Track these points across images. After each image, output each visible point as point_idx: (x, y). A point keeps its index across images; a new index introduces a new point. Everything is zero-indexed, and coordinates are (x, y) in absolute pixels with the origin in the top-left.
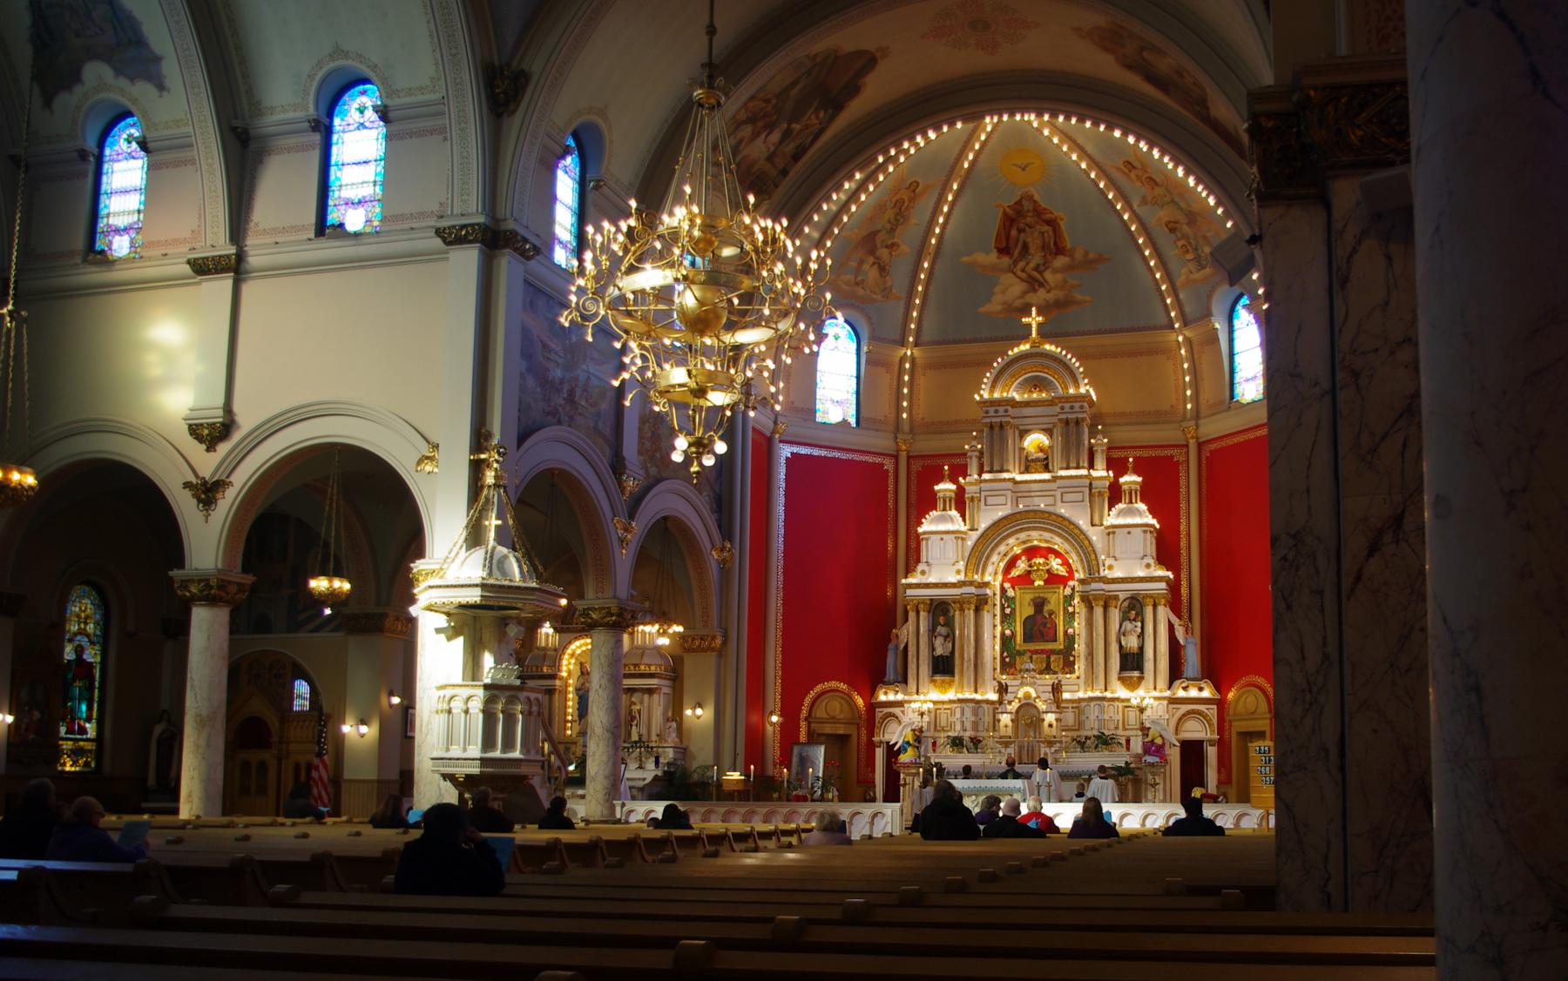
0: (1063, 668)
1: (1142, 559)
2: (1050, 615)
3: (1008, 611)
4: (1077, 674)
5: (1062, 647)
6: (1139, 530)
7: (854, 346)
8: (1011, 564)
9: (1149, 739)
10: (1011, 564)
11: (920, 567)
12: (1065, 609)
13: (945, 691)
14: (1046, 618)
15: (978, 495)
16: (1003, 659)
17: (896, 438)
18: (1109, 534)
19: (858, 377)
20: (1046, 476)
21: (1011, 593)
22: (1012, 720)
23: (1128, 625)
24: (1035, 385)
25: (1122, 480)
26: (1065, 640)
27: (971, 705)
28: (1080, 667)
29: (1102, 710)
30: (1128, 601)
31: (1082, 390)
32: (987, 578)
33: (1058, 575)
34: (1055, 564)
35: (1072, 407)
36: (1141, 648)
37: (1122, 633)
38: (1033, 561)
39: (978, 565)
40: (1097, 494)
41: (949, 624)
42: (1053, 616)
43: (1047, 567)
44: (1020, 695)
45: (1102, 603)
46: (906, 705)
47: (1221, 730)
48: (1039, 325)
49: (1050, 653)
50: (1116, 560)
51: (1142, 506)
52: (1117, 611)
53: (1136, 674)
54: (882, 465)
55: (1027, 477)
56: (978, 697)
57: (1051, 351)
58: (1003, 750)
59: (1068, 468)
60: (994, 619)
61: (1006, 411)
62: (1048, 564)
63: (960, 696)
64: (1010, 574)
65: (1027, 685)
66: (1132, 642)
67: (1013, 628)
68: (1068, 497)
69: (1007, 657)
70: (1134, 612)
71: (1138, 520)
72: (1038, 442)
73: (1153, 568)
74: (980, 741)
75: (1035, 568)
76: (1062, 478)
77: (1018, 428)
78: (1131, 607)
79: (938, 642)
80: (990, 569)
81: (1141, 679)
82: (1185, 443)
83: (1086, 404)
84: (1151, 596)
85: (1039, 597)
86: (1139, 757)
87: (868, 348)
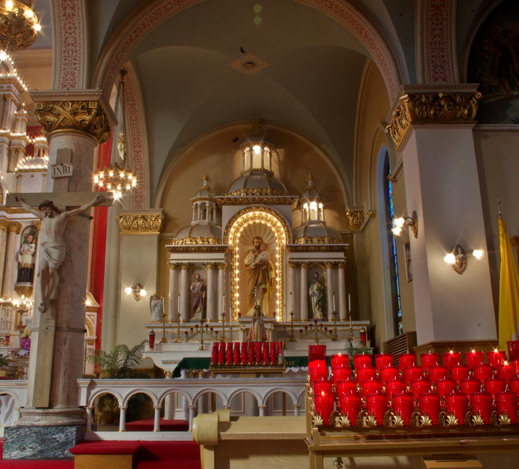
6: (40, 174)
23: (26, 247)
36: (34, 265)
52: (19, 236)
53: (28, 284)
66: (27, 260)
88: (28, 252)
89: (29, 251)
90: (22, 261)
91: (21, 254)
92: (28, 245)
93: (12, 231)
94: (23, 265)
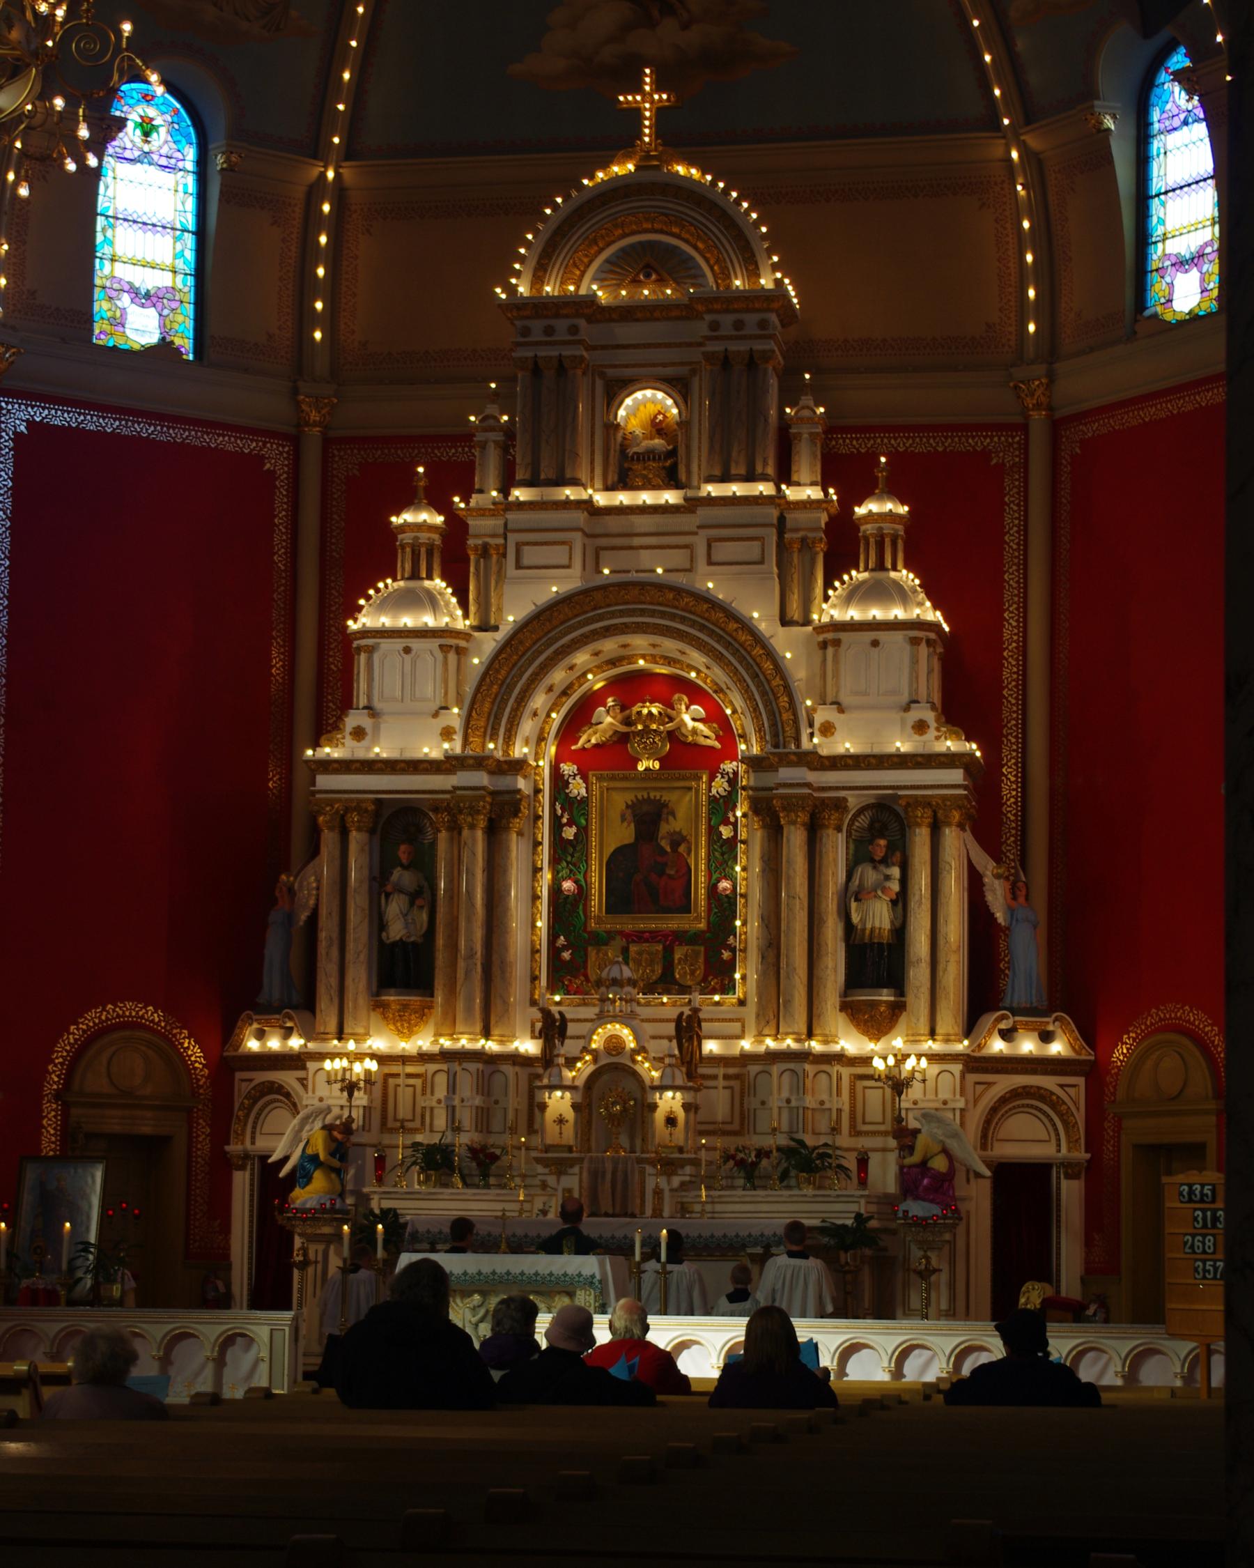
0: (705, 979)
1: (907, 709)
2: (675, 844)
3: (569, 833)
4: (739, 992)
5: (702, 925)
6: (899, 637)
7: (191, 153)
8: (579, 717)
9: (916, 1158)
10: (579, 717)
11: (352, 720)
12: (713, 832)
13: (407, 1031)
14: (662, 852)
15: (501, 541)
16: (554, 952)
17: (295, 391)
18: (824, 645)
19: (200, 233)
20: (670, 497)
21: (578, 788)
22: (575, 1106)
23: (869, 875)
24: (648, 266)
25: (860, 511)
26: (709, 909)
27: (473, 1067)
28: (746, 976)
29: (799, 1086)
30: (868, 814)
31: (766, 282)
32: (520, 750)
33: (695, 745)
34: (690, 718)
35: (739, 325)
36: (900, 932)
37: (852, 894)
38: (635, 709)
39: (498, 718)
40: (796, 546)
41: (424, 863)
42: (682, 849)
43: (670, 726)
44: (597, 1042)
45: (803, 817)
46: (312, 1066)
47: (1093, 1140)
48: (661, 113)
49: (674, 939)
50: (841, 710)
51: (906, 577)
52: (841, 838)
53: (886, 996)
54: (261, 459)
55: (623, 498)
56: (492, 1046)
57: (689, 179)
58: (552, 1180)
59: (725, 478)
60: (534, 852)
61: (574, 330)
62: (671, 719)
63: (446, 1043)
64: (576, 742)
65: (615, 1019)
66: (878, 916)
67: (580, 877)
68: (724, 551)
69: (565, 948)
70: (883, 842)
71: (898, 613)
72: (652, 409)
73: (932, 733)
74: (495, 1158)
75: (640, 727)
76: (710, 501)
77: (602, 375)
78: (877, 830)
79: (394, 908)
80: (527, 727)
81: (898, 1009)
82: (1018, 419)
83: (773, 318)
84: (926, 803)
85: (648, 801)
86: (888, 1202)
87: (227, 161)
88: (879, 893)
89: (884, 890)
90: (863, 921)
91: (856, 900)
92: (875, 868)
93: (827, 827)
94: (868, 932)
